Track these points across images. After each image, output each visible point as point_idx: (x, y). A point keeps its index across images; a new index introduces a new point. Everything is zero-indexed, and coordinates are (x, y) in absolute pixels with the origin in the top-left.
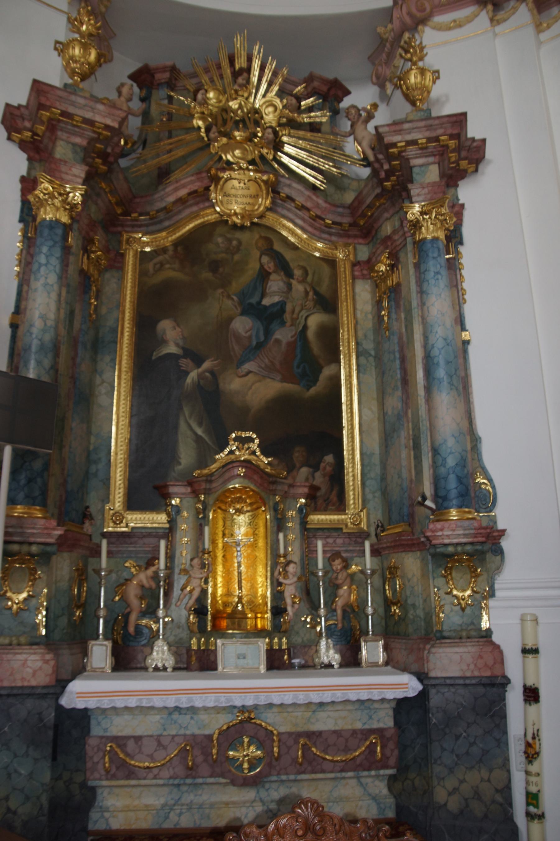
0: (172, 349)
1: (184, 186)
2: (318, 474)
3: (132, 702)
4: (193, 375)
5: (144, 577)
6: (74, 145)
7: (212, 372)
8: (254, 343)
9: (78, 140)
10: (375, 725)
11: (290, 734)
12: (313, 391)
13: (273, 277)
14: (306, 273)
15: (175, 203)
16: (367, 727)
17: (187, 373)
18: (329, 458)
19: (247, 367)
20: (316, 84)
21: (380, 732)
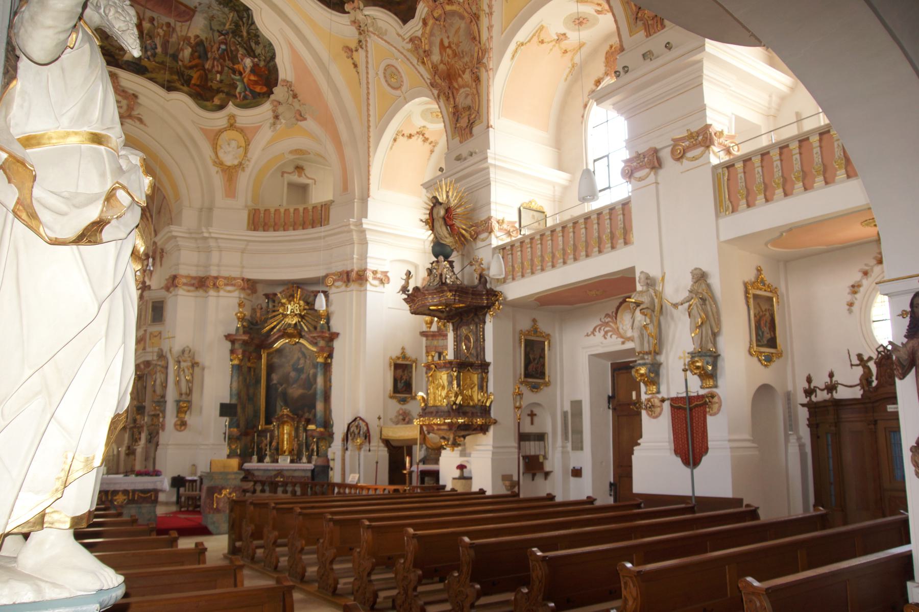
0: (275, 382)
3: (256, 468)
4: (280, 389)
14: (310, 358)
17: (278, 389)
19: (295, 386)
21: (308, 477)
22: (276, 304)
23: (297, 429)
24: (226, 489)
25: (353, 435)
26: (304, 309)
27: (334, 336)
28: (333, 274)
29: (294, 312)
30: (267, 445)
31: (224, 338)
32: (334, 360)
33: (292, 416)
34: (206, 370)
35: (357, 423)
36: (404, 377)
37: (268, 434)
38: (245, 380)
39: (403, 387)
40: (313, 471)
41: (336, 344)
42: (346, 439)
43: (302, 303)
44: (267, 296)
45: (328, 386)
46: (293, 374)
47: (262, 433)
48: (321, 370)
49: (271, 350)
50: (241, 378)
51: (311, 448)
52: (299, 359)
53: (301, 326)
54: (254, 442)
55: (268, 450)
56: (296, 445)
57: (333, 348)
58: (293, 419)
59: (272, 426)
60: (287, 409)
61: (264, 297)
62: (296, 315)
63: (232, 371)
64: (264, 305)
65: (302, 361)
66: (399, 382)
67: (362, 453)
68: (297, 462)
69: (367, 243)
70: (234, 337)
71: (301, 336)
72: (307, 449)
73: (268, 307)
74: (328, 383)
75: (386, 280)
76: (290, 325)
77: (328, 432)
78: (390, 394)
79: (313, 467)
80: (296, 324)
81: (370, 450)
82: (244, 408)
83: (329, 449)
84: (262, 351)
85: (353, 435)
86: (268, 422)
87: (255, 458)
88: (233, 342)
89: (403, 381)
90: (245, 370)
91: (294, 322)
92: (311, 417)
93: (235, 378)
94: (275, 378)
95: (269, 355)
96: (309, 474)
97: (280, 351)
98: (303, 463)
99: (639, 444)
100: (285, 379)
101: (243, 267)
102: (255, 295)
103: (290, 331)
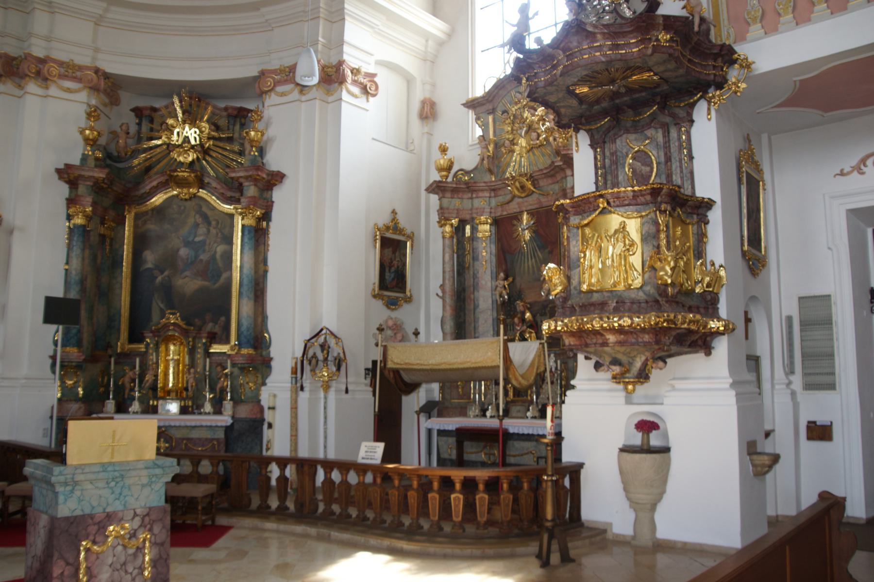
0: (150, 265)
1: (155, 180)
2: (217, 326)
4: (159, 279)
5: (131, 373)
6: (87, 185)
7: (168, 277)
8: (189, 261)
9: (88, 183)
10: (216, 437)
11: (180, 439)
12: (217, 285)
13: (201, 226)
14: (218, 223)
15: (151, 189)
16: (213, 437)
17: (156, 278)
18: (223, 319)
19: (187, 273)
20: (230, 111)
21: (218, 440)
22: (155, 126)
23: (192, 352)
24: (120, 521)
25: (314, 361)
26: (209, 139)
27: (278, 178)
28: (274, 72)
29: (189, 142)
30: (133, 381)
31: (56, 176)
32: (272, 224)
33: (184, 326)
34: (16, 234)
35: (321, 339)
36: (395, 263)
37: (138, 360)
38: (94, 258)
39: (393, 279)
40: (228, 429)
41: (278, 195)
42: (297, 371)
43: (205, 126)
44: (138, 112)
45: (261, 272)
46: (183, 252)
47: (125, 358)
48: (249, 239)
49: (143, 209)
50: (87, 252)
51: (219, 386)
52: (197, 225)
53: (203, 168)
54: (110, 374)
55: (137, 389)
56: (191, 381)
57: (273, 202)
58: (185, 333)
59: (143, 346)
60: (173, 314)
61: (133, 114)
62: (193, 147)
63: (70, 239)
64: (133, 129)
65: (202, 230)
66: (387, 270)
67: (332, 395)
68: (193, 413)
69: (344, 19)
70: (77, 173)
71: (202, 185)
72: (212, 390)
73: (139, 132)
74: (261, 266)
75: (373, 88)
76: (181, 164)
77: (261, 356)
78: (374, 290)
79: (229, 421)
80: (192, 162)
81: (347, 391)
82: (91, 310)
83: (263, 388)
84: (127, 208)
85: (314, 361)
86: (135, 336)
87: (110, 405)
88: (73, 183)
89: (393, 269)
90: (94, 239)
91: (190, 159)
92: (217, 329)
93: (76, 251)
94: (150, 258)
95: (137, 217)
96: (221, 435)
97: (159, 211)
98: (206, 414)
99: (573, 387)
100: (170, 261)
101: (97, 50)
102: (115, 108)
103: (183, 174)
